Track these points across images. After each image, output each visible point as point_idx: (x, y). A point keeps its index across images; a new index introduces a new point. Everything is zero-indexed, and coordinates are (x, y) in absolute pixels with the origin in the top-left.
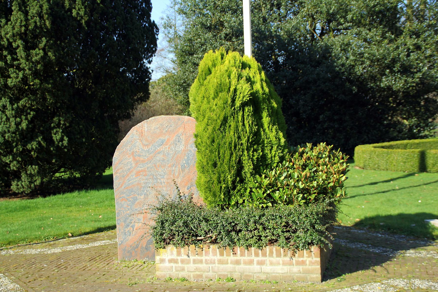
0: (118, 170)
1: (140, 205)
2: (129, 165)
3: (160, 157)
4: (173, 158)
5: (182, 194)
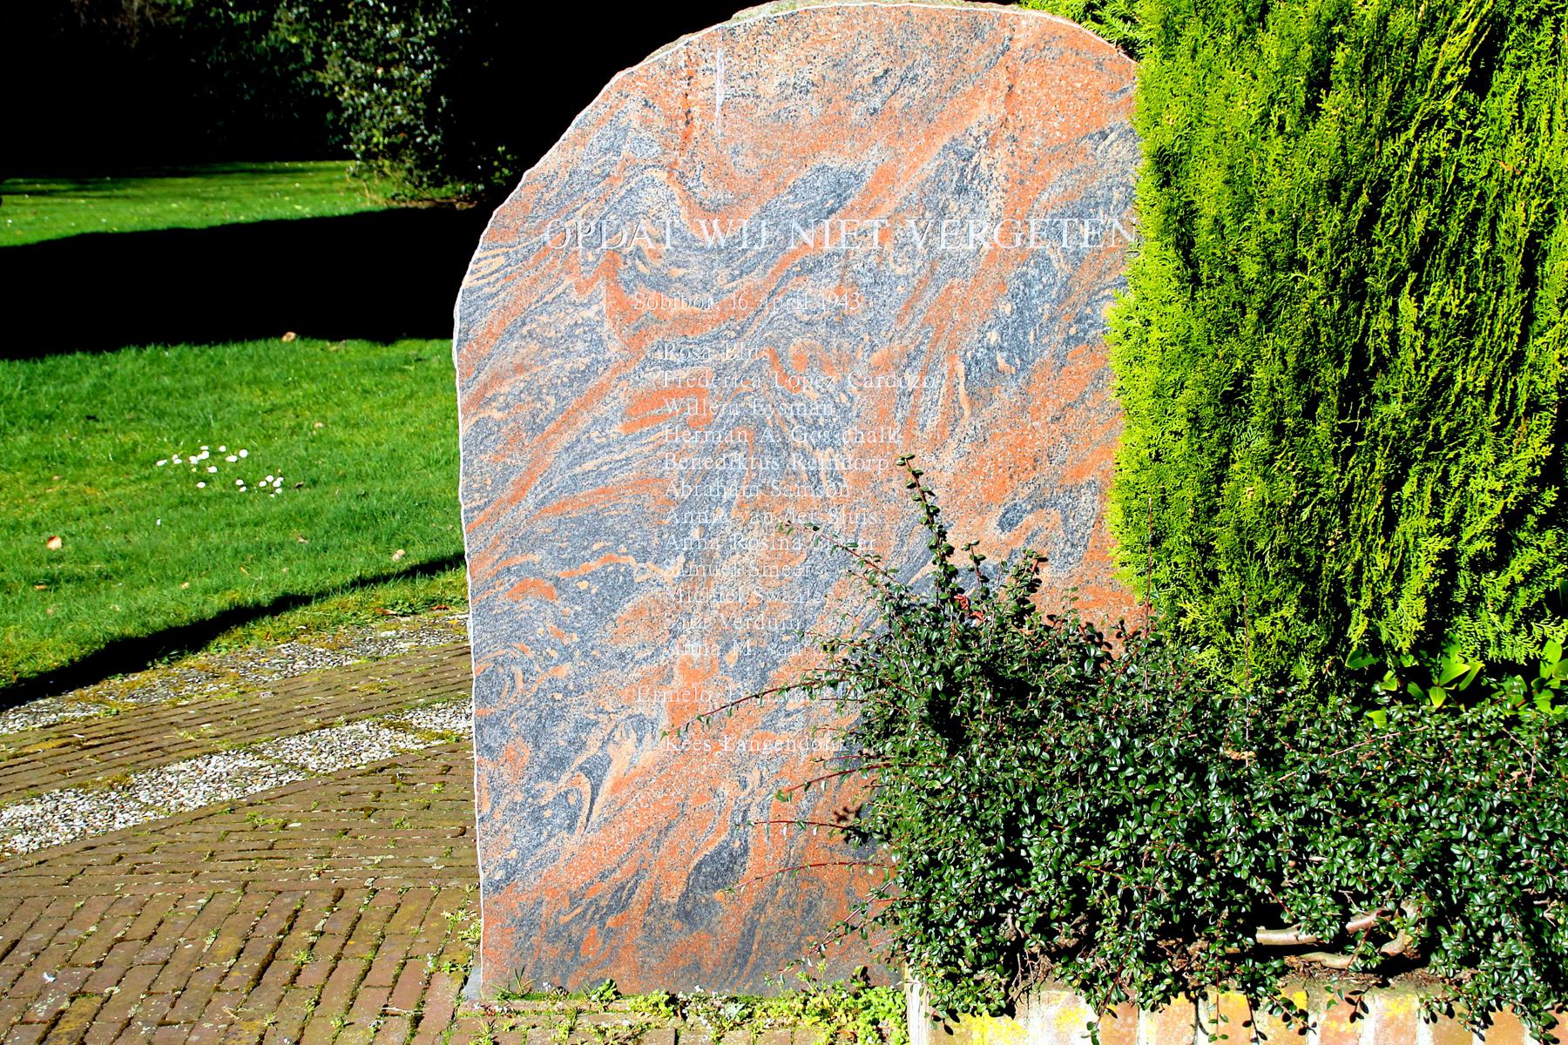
0: (498, 378)
1: (652, 624)
2: (580, 346)
3: (820, 294)
4: (909, 306)
5: (960, 560)
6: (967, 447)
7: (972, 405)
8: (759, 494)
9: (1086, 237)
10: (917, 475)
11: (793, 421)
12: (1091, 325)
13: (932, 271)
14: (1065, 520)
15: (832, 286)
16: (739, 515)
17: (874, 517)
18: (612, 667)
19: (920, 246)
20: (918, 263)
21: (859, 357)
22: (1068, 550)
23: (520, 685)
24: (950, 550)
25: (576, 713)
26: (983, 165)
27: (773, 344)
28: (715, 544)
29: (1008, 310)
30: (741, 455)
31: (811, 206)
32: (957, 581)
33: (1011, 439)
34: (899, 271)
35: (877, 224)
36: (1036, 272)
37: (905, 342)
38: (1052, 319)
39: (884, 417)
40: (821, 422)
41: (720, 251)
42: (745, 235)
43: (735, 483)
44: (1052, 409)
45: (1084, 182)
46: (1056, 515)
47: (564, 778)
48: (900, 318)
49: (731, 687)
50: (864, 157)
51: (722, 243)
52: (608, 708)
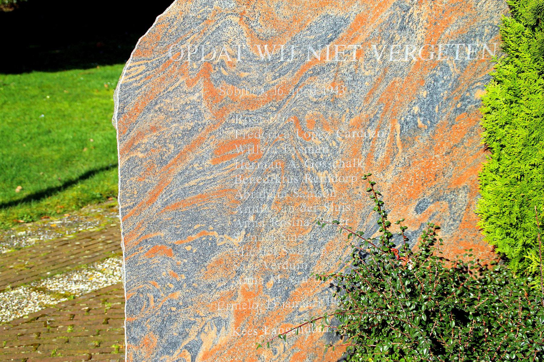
0: (141, 135)
1: (226, 268)
2: (188, 116)
3: (323, 86)
4: (372, 92)
5: (395, 229)
6: (400, 169)
7: (403, 146)
8: (287, 196)
9: (469, 54)
10: (372, 185)
11: (306, 156)
12: (469, 102)
13: (385, 73)
14: (450, 207)
15: (330, 82)
16: (276, 208)
17: (349, 207)
18: (204, 292)
19: (378, 59)
20: (377, 69)
21: (343, 121)
22: (451, 223)
23: (152, 304)
24: (389, 225)
25: (183, 318)
26: (415, 14)
27: (296, 114)
28: (262, 224)
29: (425, 94)
30: (278, 175)
31: (320, 37)
32: (392, 240)
33: (424, 164)
34: (367, 73)
35: (355, 47)
36: (440, 73)
37: (368, 112)
38: (448, 99)
39: (356, 153)
40: (322, 157)
41: (268, 62)
42: (282, 54)
43: (274, 191)
44: (446, 148)
45: (469, 23)
46: (445, 204)
47: (176, 353)
48: (366, 99)
49: (269, 300)
50: (350, 10)
51: (270, 58)
52: (201, 314)
